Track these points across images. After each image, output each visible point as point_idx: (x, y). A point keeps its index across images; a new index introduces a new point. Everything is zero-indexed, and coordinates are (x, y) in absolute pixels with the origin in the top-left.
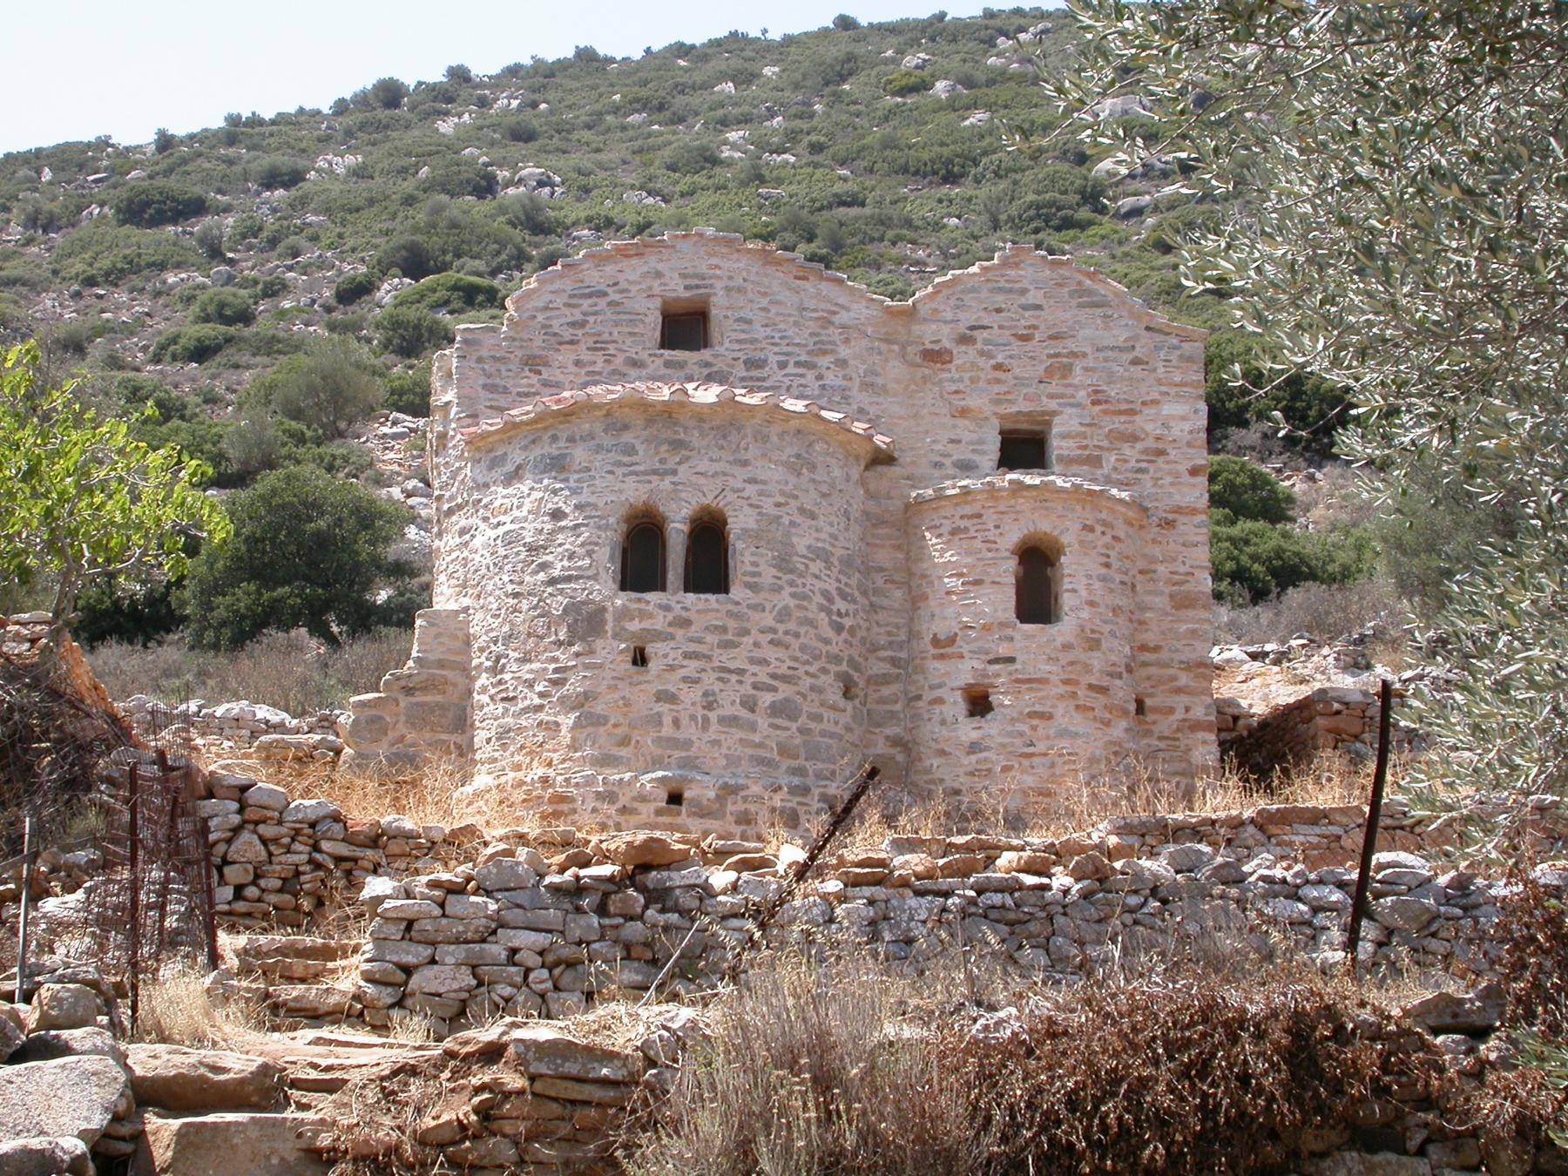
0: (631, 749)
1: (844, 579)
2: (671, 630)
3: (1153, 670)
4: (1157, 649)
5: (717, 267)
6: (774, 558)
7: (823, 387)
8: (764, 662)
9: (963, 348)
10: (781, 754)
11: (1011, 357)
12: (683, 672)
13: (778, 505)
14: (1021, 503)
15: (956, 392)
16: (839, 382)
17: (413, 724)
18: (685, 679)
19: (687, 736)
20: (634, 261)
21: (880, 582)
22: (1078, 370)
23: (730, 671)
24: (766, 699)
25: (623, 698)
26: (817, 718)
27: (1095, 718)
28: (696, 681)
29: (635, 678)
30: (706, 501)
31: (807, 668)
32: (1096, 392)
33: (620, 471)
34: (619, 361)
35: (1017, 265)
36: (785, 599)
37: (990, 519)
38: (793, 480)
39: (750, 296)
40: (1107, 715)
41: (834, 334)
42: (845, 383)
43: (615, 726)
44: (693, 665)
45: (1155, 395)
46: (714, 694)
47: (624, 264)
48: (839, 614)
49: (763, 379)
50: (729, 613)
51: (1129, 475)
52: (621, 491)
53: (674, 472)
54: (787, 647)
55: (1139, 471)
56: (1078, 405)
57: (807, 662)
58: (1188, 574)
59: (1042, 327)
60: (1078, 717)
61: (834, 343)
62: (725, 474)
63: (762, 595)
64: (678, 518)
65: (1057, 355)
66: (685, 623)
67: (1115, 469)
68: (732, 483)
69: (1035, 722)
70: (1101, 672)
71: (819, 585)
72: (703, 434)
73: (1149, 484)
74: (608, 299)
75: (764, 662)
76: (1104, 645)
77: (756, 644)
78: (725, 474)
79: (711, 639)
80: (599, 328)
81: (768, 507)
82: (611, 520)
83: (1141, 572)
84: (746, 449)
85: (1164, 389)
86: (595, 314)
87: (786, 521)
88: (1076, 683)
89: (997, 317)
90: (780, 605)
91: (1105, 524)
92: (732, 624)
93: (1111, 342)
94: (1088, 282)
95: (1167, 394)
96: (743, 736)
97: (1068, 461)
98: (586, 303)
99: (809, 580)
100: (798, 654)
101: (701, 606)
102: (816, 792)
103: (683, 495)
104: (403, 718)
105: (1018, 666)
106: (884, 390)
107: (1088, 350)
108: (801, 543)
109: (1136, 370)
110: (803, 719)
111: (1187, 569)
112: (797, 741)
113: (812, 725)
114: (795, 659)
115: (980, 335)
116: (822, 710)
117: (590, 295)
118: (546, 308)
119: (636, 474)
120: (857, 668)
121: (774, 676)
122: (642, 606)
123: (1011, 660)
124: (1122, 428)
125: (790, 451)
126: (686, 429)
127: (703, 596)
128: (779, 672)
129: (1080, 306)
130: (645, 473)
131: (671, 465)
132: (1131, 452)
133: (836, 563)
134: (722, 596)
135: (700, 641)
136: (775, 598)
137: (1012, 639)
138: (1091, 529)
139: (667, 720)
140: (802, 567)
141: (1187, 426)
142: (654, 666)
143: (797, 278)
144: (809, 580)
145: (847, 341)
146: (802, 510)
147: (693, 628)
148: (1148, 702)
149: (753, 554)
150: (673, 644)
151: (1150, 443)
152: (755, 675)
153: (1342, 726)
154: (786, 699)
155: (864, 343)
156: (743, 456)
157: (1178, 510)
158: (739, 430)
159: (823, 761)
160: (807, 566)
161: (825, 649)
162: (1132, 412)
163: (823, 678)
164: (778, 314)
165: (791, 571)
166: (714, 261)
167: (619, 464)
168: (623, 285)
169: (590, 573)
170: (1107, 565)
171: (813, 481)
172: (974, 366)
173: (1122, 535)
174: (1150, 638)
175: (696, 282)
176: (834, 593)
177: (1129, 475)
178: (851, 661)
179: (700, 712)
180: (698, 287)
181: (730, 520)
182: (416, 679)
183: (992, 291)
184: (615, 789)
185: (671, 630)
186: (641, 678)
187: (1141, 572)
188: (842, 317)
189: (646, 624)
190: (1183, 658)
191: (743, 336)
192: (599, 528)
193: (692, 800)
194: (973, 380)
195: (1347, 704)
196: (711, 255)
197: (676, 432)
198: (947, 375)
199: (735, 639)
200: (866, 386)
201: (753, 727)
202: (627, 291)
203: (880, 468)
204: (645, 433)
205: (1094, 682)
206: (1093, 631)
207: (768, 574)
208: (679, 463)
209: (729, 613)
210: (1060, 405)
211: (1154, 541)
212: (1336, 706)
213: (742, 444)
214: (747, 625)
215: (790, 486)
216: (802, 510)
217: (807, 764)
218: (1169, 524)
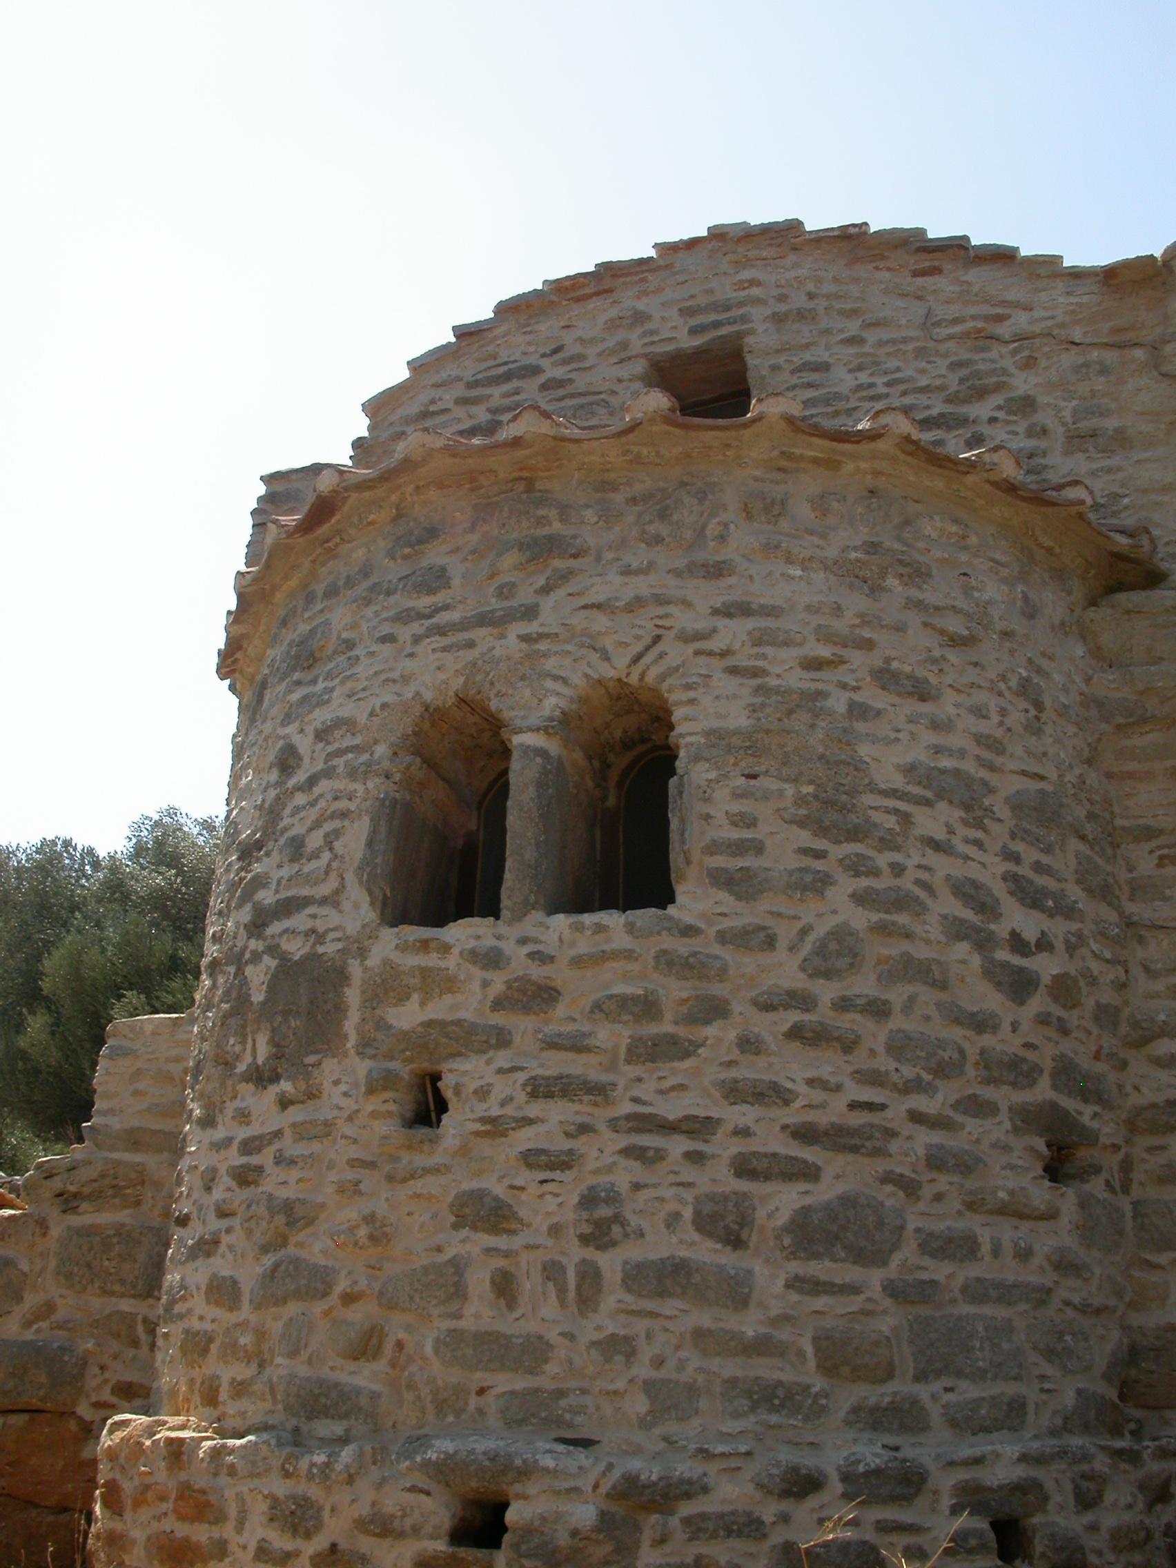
0: (381, 1365)
1: (1030, 854)
2: (498, 1019)
5: (753, 283)
6: (800, 800)
8: (772, 1094)
10: (828, 1367)
12: (525, 1139)
13: (814, 664)
17: (69, 1276)
18: (531, 1158)
19: (530, 1326)
20: (590, 305)
21: (1146, 866)
25: (370, 1219)
26: (963, 1247)
28: (564, 1162)
29: (406, 1157)
30: (608, 672)
31: (919, 1102)
33: (405, 634)
38: (856, 602)
39: (824, 323)
41: (1000, 357)
42: (1031, 443)
43: (349, 1299)
44: (558, 1113)
46: (613, 1197)
47: (576, 309)
48: (1017, 943)
50: (667, 961)
52: (406, 679)
53: (530, 612)
54: (849, 1045)
57: (907, 1089)
61: (1005, 372)
62: (661, 600)
63: (765, 904)
64: (533, 721)
68: (682, 619)
71: (943, 866)
72: (608, 516)
74: (542, 379)
75: (772, 1094)
77: (749, 1044)
78: (661, 600)
82: (381, 750)
84: (722, 538)
87: (838, 702)
90: (821, 929)
96: (704, 1318)
98: (496, 392)
99: (913, 857)
100: (885, 1063)
101: (584, 946)
102: (945, 1482)
103: (550, 664)
104: (53, 1263)
106: (1122, 440)
110: (908, 1252)
112: (885, 1325)
113: (940, 1271)
114: (875, 1079)
116: (975, 1224)
117: (507, 377)
119: (441, 631)
120: (1090, 1091)
121: (805, 1134)
122: (431, 960)
126: (565, 512)
127: (588, 919)
128: (823, 1119)
130: (463, 626)
131: (525, 595)
133: (1002, 811)
134: (645, 916)
135: (577, 1045)
136: (809, 911)
139: (479, 1280)
140: (891, 822)
142: (454, 1125)
143: (916, 274)
144: (913, 857)
146: (886, 677)
147: (561, 1010)
149: (737, 795)
150: (503, 1059)
152: (743, 1132)
154: (847, 1201)
155: (1069, 359)
156: (709, 553)
158: (701, 496)
159: (980, 1376)
160: (905, 818)
161: (973, 1044)
163: (973, 1125)
164: (881, 343)
165: (854, 834)
166: (746, 274)
167: (405, 617)
168: (573, 349)
169: (325, 889)
171: (920, 605)
175: (714, 317)
176: (999, 889)
178: (1065, 1073)
179: (574, 1254)
180: (716, 325)
181: (678, 714)
182: (85, 1174)
184: (314, 1491)
185: (498, 1019)
186: (420, 1160)
189: (439, 1009)
192: (352, 774)
193: (528, 1531)
197: (542, 521)
199: (682, 1031)
200: (1078, 440)
202: (580, 357)
203: (1124, 599)
204: (474, 538)
208: (546, 590)
209: (667, 961)
213: (712, 529)
214: (719, 990)
215: (849, 617)
216: (886, 677)
217: (924, 1392)
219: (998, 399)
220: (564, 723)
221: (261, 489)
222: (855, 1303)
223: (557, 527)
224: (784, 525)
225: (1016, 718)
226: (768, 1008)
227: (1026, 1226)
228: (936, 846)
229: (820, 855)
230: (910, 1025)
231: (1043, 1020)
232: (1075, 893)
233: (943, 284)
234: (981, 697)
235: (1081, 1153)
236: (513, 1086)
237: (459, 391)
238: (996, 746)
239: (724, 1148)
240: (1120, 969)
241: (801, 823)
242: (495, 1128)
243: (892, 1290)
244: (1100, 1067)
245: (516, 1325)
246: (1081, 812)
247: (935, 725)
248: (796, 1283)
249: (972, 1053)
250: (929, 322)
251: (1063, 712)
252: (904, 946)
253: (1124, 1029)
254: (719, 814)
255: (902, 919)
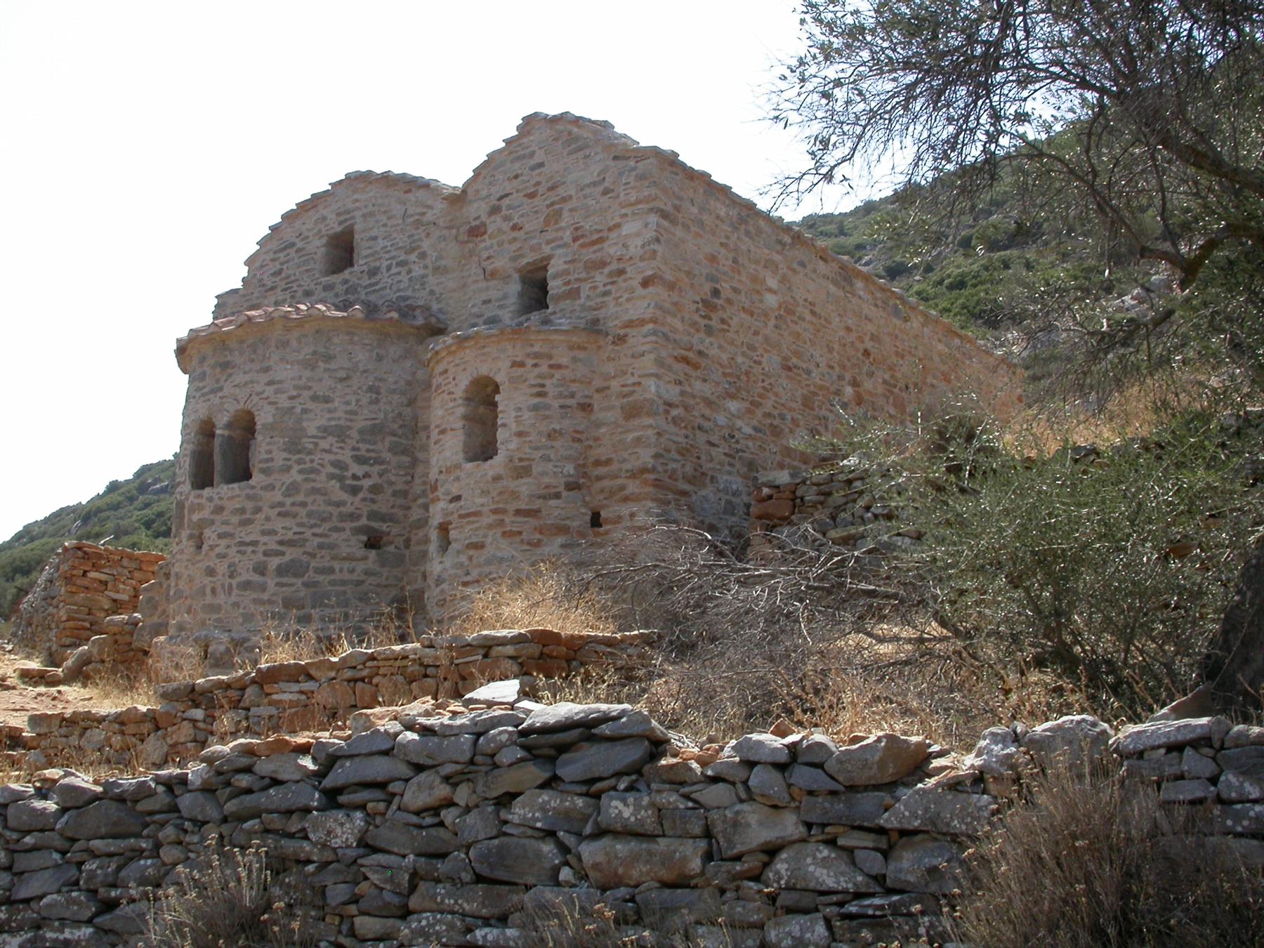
1: (362, 446)
3: (606, 483)
4: (608, 462)
5: (357, 200)
7: (410, 280)
8: (274, 532)
9: (493, 218)
11: (522, 216)
12: (217, 550)
13: (292, 398)
14: (469, 354)
15: (488, 258)
16: (422, 272)
22: (566, 214)
23: (248, 544)
24: (274, 562)
27: (522, 542)
32: (577, 229)
33: (198, 395)
34: (300, 294)
35: (529, 133)
36: (295, 476)
37: (452, 370)
38: (307, 373)
40: (538, 536)
44: (224, 542)
45: (618, 220)
48: (355, 477)
49: (376, 284)
50: (248, 497)
51: (599, 300)
52: (196, 411)
54: (295, 516)
55: (606, 294)
56: (565, 245)
57: (312, 527)
58: (634, 384)
59: (544, 183)
60: (504, 543)
61: (421, 240)
62: (252, 382)
63: (275, 476)
65: (552, 204)
66: (219, 510)
67: (588, 297)
68: (258, 388)
69: (471, 552)
70: (531, 496)
71: (328, 457)
73: (612, 304)
75: (274, 532)
76: (535, 471)
77: (268, 519)
78: (252, 382)
79: (235, 519)
80: (291, 272)
81: (284, 402)
83: (597, 391)
85: (624, 211)
86: (287, 262)
87: (298, 410)
88: (504, 511)
89: (515, 183)
90: (288, 482)
91: (537, 356)
92: (249, 505)
93: (587, 181)
94: (576, 130)
95: (626, 215)
96: (255, 596)
97: (560, 298)
98: (282, 255)
99: (317, 457)
100: (305, 520)
105: (462, 503)
107: (572, 192)
108: (311, 428)
109: (605, 200)
110: (311, 572)
111: (636, 379)
112: (302, 594)
113: (320, 578)
114: (301, 525)
115: (506, 201)
118: (262, 266)
119: (203, 395)
121: (281, 543)
123: (458, 498)
124: (593, 257)
125: (307, 350)
128: (286, 538)
129: (570, 153)
132: (600, 278)
134: (244, 484)
135: (226, 523)
137: (458, 479)
138: (522, 365)
139: (208, 591)
141: (639, 242)
142: (205, 547)
143: (406, 192)
145: (428, 235)
147: (225, 513)
148: (602, 513)
149: (269, 444)
151: (614, 266)
152: (265, 544)
153: (770, 511)
154: (292, 561)
155: (438, 233)
156: (266, 364)
157: (630, 324)
160: (316, 444)
162: (601, 240)
163: (335, 535)
165: (299, 452)
166: (356, 196)
168: (306, 234)
170: (540, 395)
171: (329, 370)
172: (499, 230)
173: (564, 361)
174: (601, 452)
176: (349, 461)
177: (599, 300)
178: (373, 515)
180: (346, 220)
183: (512, 162)
186: (199, 558)
187: (597, 391)
188: (429, 216)
190: (629, 466)
191: (369, 251)
194: (500, 244)
195: (778, 487)
196: (355, 192)
198: (483, 245)
200: (437, 270)
201: (263, 588)
205: (523, 507)
206: (521, 460)
207: (279, 457)
209: (248, 497)
210: (552, 249)
211: (610, 359)
212: (766, 491)
214: (260, 504)
215: (304, 380)
216: (315, 398)
218: (621, 339)
219: (416, 253)
220: (229, 426)
221: (215, 301)
222: (294, 589)
223: (229, 358)
224: (288, 350)
225: (365, 400)
226: (272, 507)
227: (354, 563)
228: (324, 451)
229: (289, 460)
230: (315, 508)
231: (364, 500)
232: (387, 456)
233: (411, 196)
234: (348, 398)
235: (385, 539)
236: (214, 536)
237: (271, 256)
238: (355, 413)
239: (261, 548)
240: (409, 478)
241: (284, 450)
242: (212, 548)
243: (304, 584)
244: (394, 511)
245: (216, 601)
246: (396, 426)
247: (330, 411)
248: (277, 584)
249: (335, 514)
250: (405, 216)
251: (393, 391)
252: (313, 484)
253: (410, 496)
254: (263, 451)
255: (312, 476)
